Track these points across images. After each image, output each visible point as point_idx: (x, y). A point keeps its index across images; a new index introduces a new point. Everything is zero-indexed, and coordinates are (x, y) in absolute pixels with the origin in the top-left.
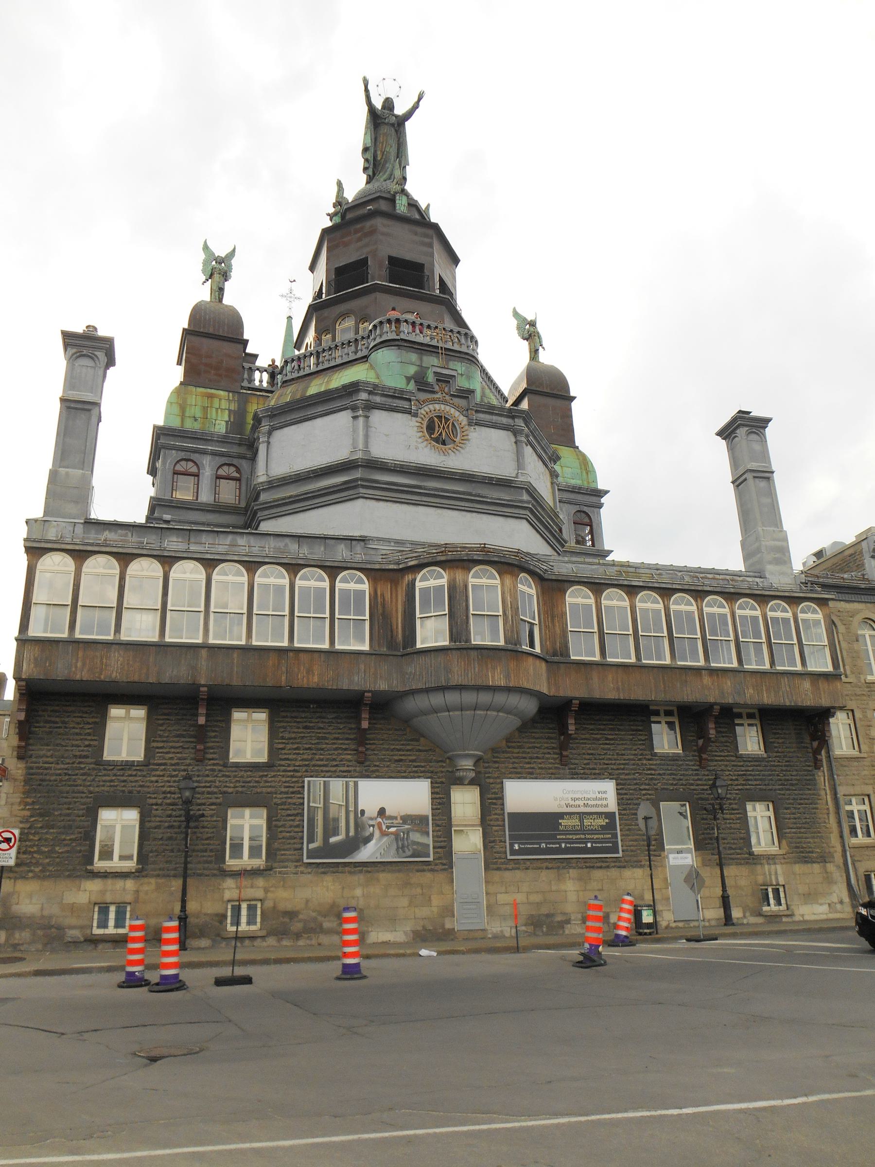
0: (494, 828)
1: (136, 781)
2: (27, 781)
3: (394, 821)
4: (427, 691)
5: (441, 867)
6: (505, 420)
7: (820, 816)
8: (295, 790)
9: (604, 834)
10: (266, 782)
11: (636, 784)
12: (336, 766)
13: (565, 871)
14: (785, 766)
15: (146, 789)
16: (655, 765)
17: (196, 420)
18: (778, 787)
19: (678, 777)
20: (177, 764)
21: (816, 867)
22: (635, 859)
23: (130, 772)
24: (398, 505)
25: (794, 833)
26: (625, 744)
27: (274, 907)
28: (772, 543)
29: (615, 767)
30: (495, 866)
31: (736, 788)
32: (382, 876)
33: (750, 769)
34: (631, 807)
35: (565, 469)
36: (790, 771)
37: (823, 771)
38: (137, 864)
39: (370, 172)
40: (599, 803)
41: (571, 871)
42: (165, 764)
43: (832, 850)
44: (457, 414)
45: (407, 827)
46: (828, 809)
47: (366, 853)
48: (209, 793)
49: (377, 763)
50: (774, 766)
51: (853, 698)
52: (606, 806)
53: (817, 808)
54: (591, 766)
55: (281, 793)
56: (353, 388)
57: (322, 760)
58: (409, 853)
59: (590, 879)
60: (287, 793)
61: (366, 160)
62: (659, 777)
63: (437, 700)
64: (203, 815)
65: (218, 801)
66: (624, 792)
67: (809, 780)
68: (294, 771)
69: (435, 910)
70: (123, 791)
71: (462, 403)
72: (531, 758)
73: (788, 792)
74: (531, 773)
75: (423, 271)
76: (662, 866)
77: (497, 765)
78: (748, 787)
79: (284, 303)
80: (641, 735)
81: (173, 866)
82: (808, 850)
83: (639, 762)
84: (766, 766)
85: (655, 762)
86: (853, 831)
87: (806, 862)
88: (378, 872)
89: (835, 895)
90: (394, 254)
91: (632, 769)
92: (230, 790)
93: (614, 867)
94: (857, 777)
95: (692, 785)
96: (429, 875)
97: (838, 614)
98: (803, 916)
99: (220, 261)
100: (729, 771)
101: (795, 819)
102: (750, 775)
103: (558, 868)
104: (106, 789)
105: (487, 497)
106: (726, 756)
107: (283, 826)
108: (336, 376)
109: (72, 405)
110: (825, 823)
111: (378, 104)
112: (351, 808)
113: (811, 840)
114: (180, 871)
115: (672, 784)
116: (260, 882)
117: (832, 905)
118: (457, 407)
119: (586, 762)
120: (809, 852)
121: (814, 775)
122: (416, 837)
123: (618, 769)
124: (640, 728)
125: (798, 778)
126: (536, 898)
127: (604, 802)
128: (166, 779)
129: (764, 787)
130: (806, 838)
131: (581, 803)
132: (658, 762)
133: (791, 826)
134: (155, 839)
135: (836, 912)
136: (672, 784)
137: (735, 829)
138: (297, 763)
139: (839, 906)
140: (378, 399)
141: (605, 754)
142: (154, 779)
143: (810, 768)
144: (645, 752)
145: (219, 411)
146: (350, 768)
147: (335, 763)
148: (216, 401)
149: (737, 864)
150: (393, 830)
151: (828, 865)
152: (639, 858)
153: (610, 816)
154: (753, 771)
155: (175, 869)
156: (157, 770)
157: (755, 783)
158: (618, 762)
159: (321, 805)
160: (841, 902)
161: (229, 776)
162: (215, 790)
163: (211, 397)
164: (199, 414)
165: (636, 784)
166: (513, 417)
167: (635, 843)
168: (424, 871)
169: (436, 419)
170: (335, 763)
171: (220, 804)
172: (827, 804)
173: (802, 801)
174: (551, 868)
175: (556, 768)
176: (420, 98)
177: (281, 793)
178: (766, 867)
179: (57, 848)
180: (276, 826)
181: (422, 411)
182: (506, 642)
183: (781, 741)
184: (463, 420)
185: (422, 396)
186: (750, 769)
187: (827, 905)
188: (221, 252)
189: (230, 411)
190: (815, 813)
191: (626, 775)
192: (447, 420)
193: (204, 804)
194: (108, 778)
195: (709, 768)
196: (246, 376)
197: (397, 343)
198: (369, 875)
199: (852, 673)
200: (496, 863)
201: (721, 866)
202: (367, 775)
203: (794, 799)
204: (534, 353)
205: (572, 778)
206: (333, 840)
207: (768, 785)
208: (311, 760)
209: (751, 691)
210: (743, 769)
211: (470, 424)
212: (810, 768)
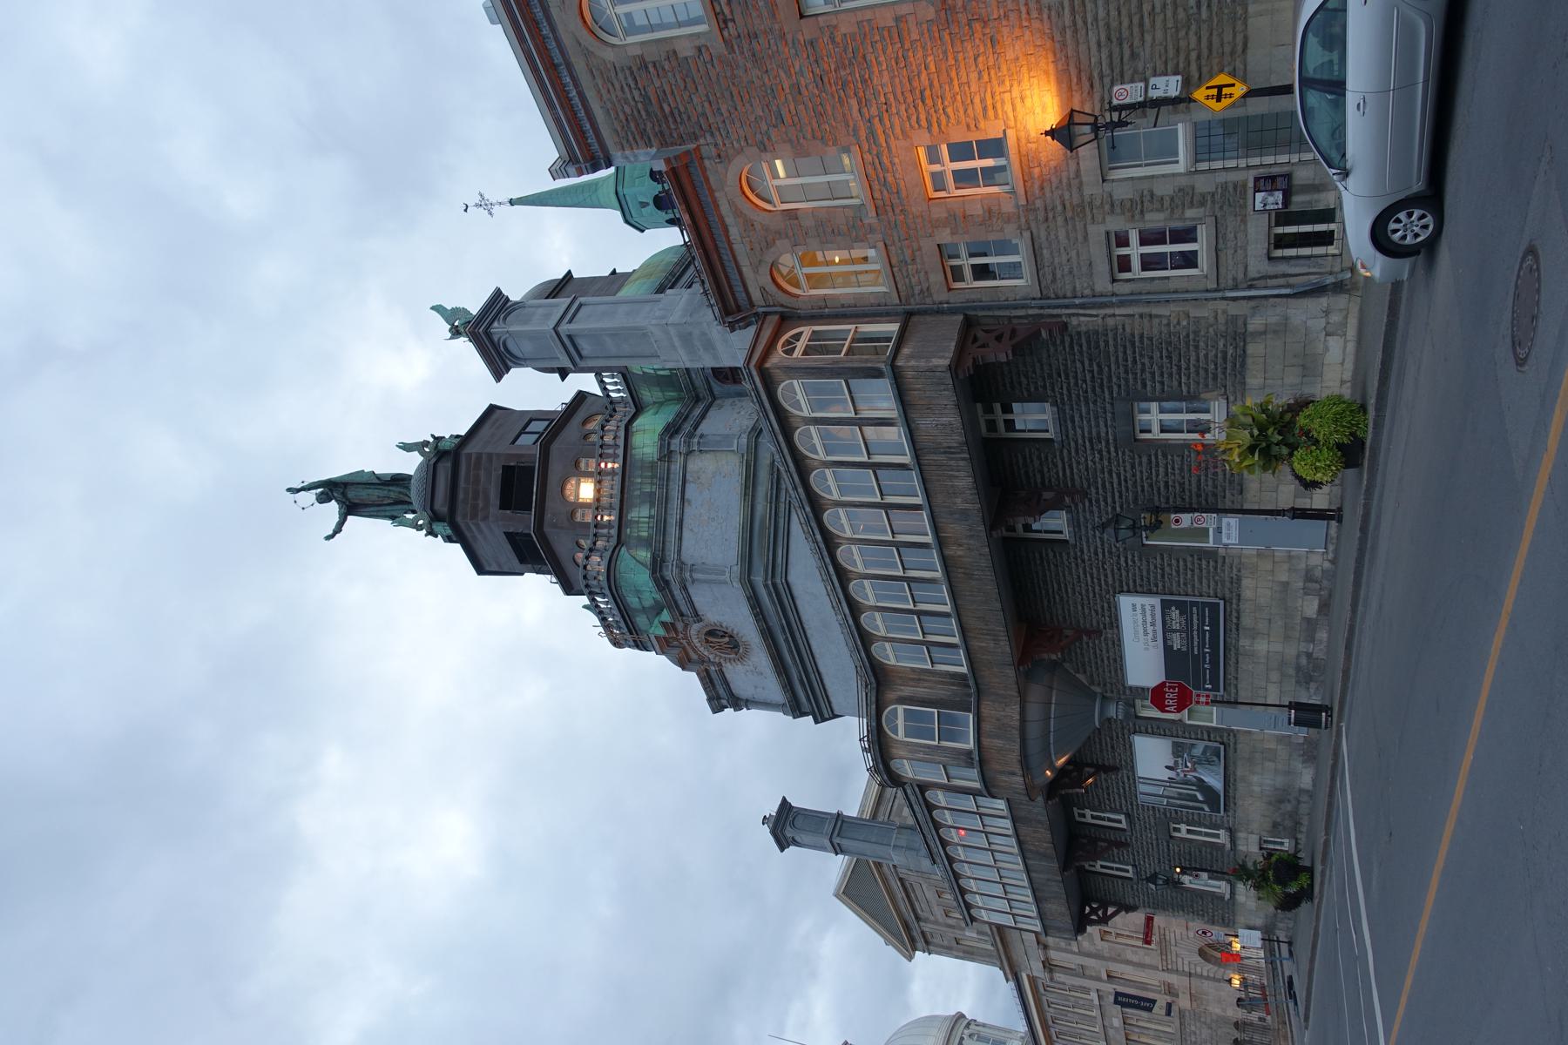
2: (1154, 908)
3: (1180, 762)
7: (1155, 331)
9: (1192, 614)
11: (1119, 569)
12: (1123, 783)
13: (1241, 649)
14: (1067, 377)
16: (1089, 547)
21: (1251, 349)
24: (827, 687)
25: (1189, 379)
26: (1063, 572)
28: (681, 352)
29: (1097, 588)
31: (1113, 454)
32: (1239, 773)
36: (1076, 372)
37: (1070, 315)
40: (1148, 613)
41: (1241, 644)
43: (1221, 319)
45: (1185, 755)
46: (1141, 316)
47: (1215, 781)
52: (1153, 606)
53: (1142, 336)
54: (1100, 610)
58: (1215, 759)
59: (1254, 628)
62: (1106, 545)
67: (1089, 342)
73: (1114, 380)
74: (1115, 660)
76: (1240, 557)
80: (1047, 555)
82: (1220, 361)
83: (1087, 563)
84: (1072, 409)
87: (1243, 364)
89: (1309, 323)
91: (1099, 571)
93: (1238, 605)
96: (1239, 746)
98: (1342, 382)
100: (1086, 460)
101: (1162, 375)
103: (1237, 654)
106: (1062, 460)
110: (1168, 325)
111: (333, 508)
112: (1168, 784)
116: (1241, 835)
117: (1330, 329)
120: (1225, 359)
121: (1079, 333)
122: (1198, 751)
123: (1100, 586)
124: (1037, 555)
126: (1275, 676)
127: (1148, 608)
129: (1109, 415)
130: (1198, 361)
131: (1150, 629)
133: (1175, 383)
135: (1344, 324)
137: (1182, 464)
138: (1124, 802)
139: (1335, 318)
140: (721, 692)
141: (1080, 594)
144: (1072, 553)
150: (1189, 764)
151: (1251, 328)
153: (1166, 605)
159: (1166, 800)
160: (1327, 313)
165: (1119, 569)
166: (667, 583)
172: (1133, 315)
173: (1130, 359)
174: (1237, 660)
181: (711, 657)
183: (1023, 379)
186: (1079, 431)
187: (1328, 338)
190: (1151, 339)
191: (1106, 576)
195: (1085, 486)
202: (1133, 768)
203: (1126, 372)
205: (1117, 627)
206: (1200, 797)
207: (1104, 408)
209: (959, 500)
210: (1080, 441)
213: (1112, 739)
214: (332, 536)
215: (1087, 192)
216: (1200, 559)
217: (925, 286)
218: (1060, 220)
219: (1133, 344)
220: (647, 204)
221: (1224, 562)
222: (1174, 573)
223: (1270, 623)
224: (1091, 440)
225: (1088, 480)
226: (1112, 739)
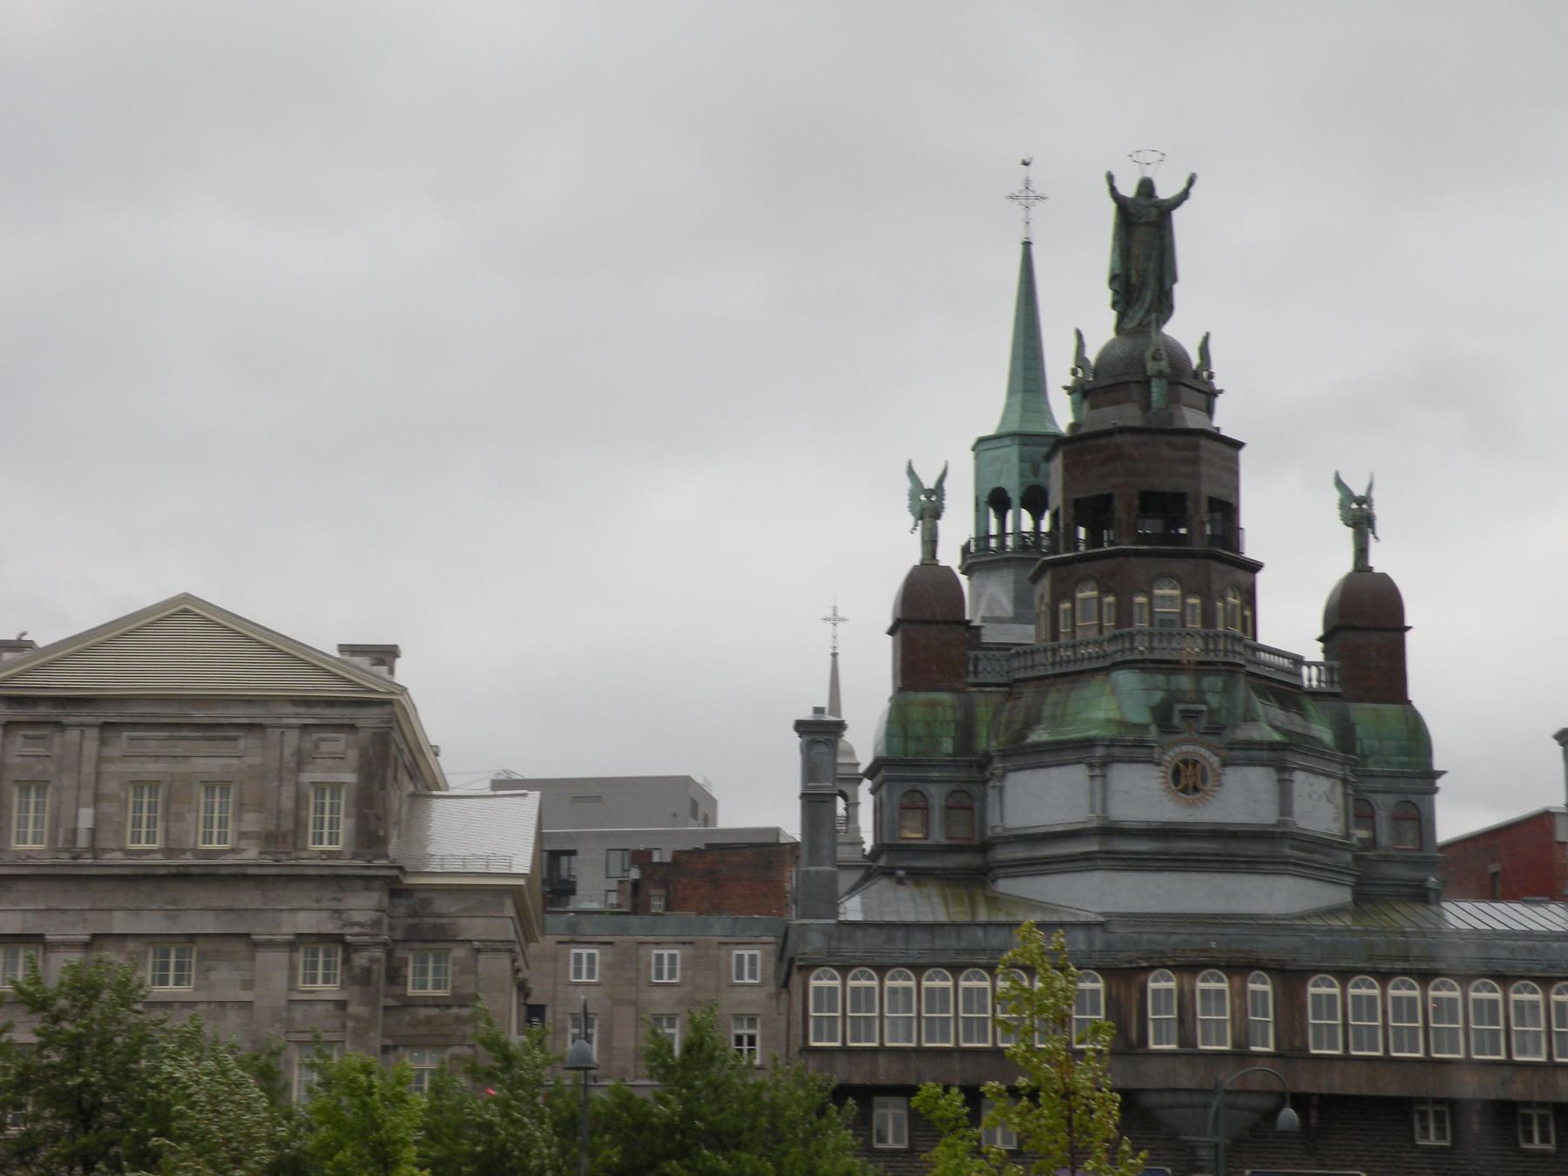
1: (903, 1167)
4: (1160, 1091)
56: (1088, 744)
61: (1116, 292)
63: (1169, 1099)
71: (1213, 740)
72: (1275, 1148)
79: (1017, 209)
99: (929, 493)
105: (1239, 856)
109: (814, 799)
111: (1128, 190)
118: (1208, 747)
148: (940, 709)
169: (1181, 765)
176: (1191, 181)
181: (1167, 758)
184: (1215, 760)
185: (1167, 739)
188: (929, 483)
192: (1195, 763)
196: (971, 668)
204: (1361, 552)
210: (1523, 1164)
214: (1113, 190)
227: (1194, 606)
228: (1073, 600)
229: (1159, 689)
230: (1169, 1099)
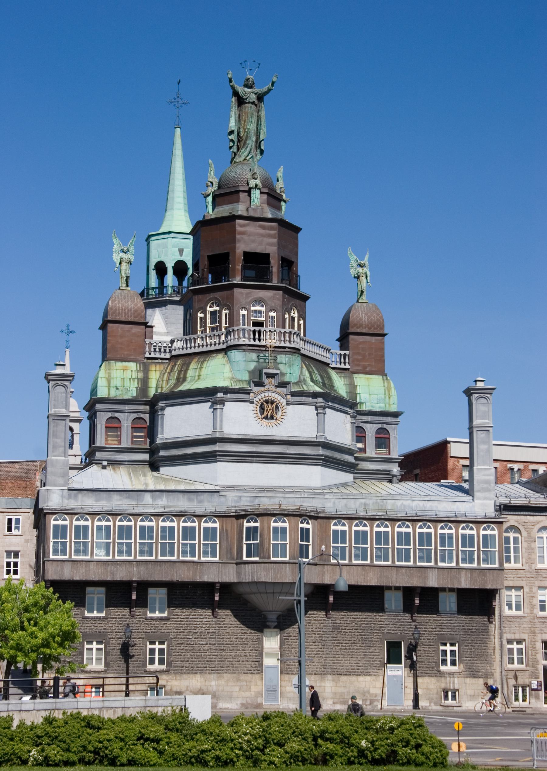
0: (287, 652)
5: (257, 671)
6: (310, 399)
7: (488, 651)
8: (181, 631)
10: (166, 627)
11: (371, 630)
14: (469, 621)
15: (107, 631)
17: (117, 389)
18: (462, 633)
19: (397, 626)
20: (122, 618)
22: (367, 671)
23: (99, 622)
27: (171, 689)
29: (359, 620)
30: (286, 672)
31: (434, 633)
32: (225, 675)
33: (445, 622)
34: (367, 642)
35: (372, 396)
38: (104, 667)
39: (235, 149)
41: (329, 676)
42: (116, 618)
43: (493, 671)
44: (279, 398)
46: (494, 647)
48: (138, 632)
49: (224, 617)
50: (462, 620)
51: (524, 579)
53: (487, 646)
54: (345, 619)
55: (174, 632)
57: (195, 615)
60: (177, 632)
64: (136, 644)
65: (142, 636)
66: (363, 634)
67: (484, 629)
68: (181, 621)
69: (253, 693)
70: (96, 632)
75: (269, 263)
77: (290, 618)
78: (442, 633)
81: (121, 668)
82: (477, 670)
83: (375, 617)
85: (384, 617)
86: (511, 661)
87: (475, 677)
88: (224, 673)
90: (248, 250)
92: (148, 631)
94: (518, 628)
95: (406, 631)
96: (250, 675)
97: (524, 524)
102: (445, 626)
103: (321, 674)
104: (88, 630)
107: (175, 649)
108: (205, 364)
109: (56, 418)
113: (480, 665)
114: (125, 671)
115: (393, 630)
118: (279, 394)
119: (342, 617)
120: (478, 672)
121: (488, 627)
123: (361, 621)
125: (477, 628)
128: (116, 625)
130: (477, 663)
132: (386, 617)
133: (467, 656)
134: (112, 655)
136: (393, 630)
138: (182, 617)
142: (111, 625)
143: (486, 623)
145: (132, 380)
146: (210, 620)
147: (202, 617)
149: (429, 676)
152: (369, 671)
154: (447, 623)
155: (123, 670)
156: (112, 621)
157: (447, 630)
158: (361, 617)
161: (147, 624)
162: (141, 631)
163: (125, 369)
164: (119, 384)
165: (371, 630)
167: (367, 662)
168: (247, 673)
169: (265, 404)
170: (202, 617)
171: (143, 638)
175: (324, 620)
177: (174, 632)
178: (448, 679)
179: (67, 659)
180: (172, 649)
182: (290, 559)
184: (284, 402)
186: (445, 622)
189: (138, 379)
191: (367, 624)
192: (273, 402)
193: (136, 638)
194: (88, 625)
196: (147, 349)
197: (244, 347)
198: (219, 675)
199: (527, 563)
200: (287, 671)
201: (416, 677)
203: (472, 640)
208: (189, 615)
211: (288, 404)
212: (486, 623)
213: (244, 616)
215: (539, 635)
216: (380, 661)
217: (508, 579)
218: (530, 626)
219: (483, 644)
220: (181, 255)
221: (379, 670)
222: (371, 651)
223: (344, 687)
224: (441, 625)
225: (421, 622)
226: (244, 616)
227: (272, 317)
228: (205, 312)
229: (252, 361)
230: (254, 589)
